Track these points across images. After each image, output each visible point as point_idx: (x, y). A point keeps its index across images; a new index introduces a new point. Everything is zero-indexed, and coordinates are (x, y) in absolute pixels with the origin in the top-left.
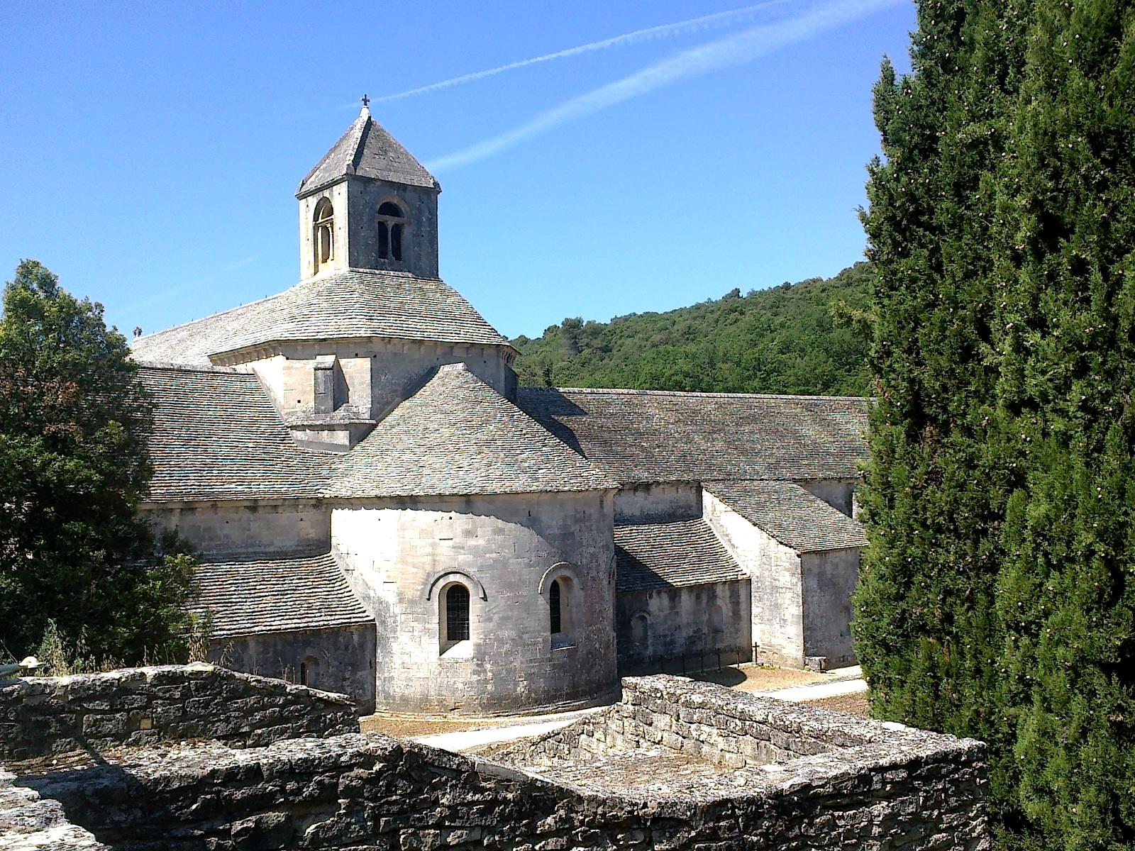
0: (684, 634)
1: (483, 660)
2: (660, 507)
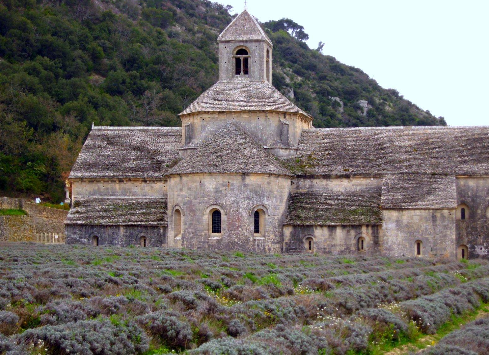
0: (338, 249)
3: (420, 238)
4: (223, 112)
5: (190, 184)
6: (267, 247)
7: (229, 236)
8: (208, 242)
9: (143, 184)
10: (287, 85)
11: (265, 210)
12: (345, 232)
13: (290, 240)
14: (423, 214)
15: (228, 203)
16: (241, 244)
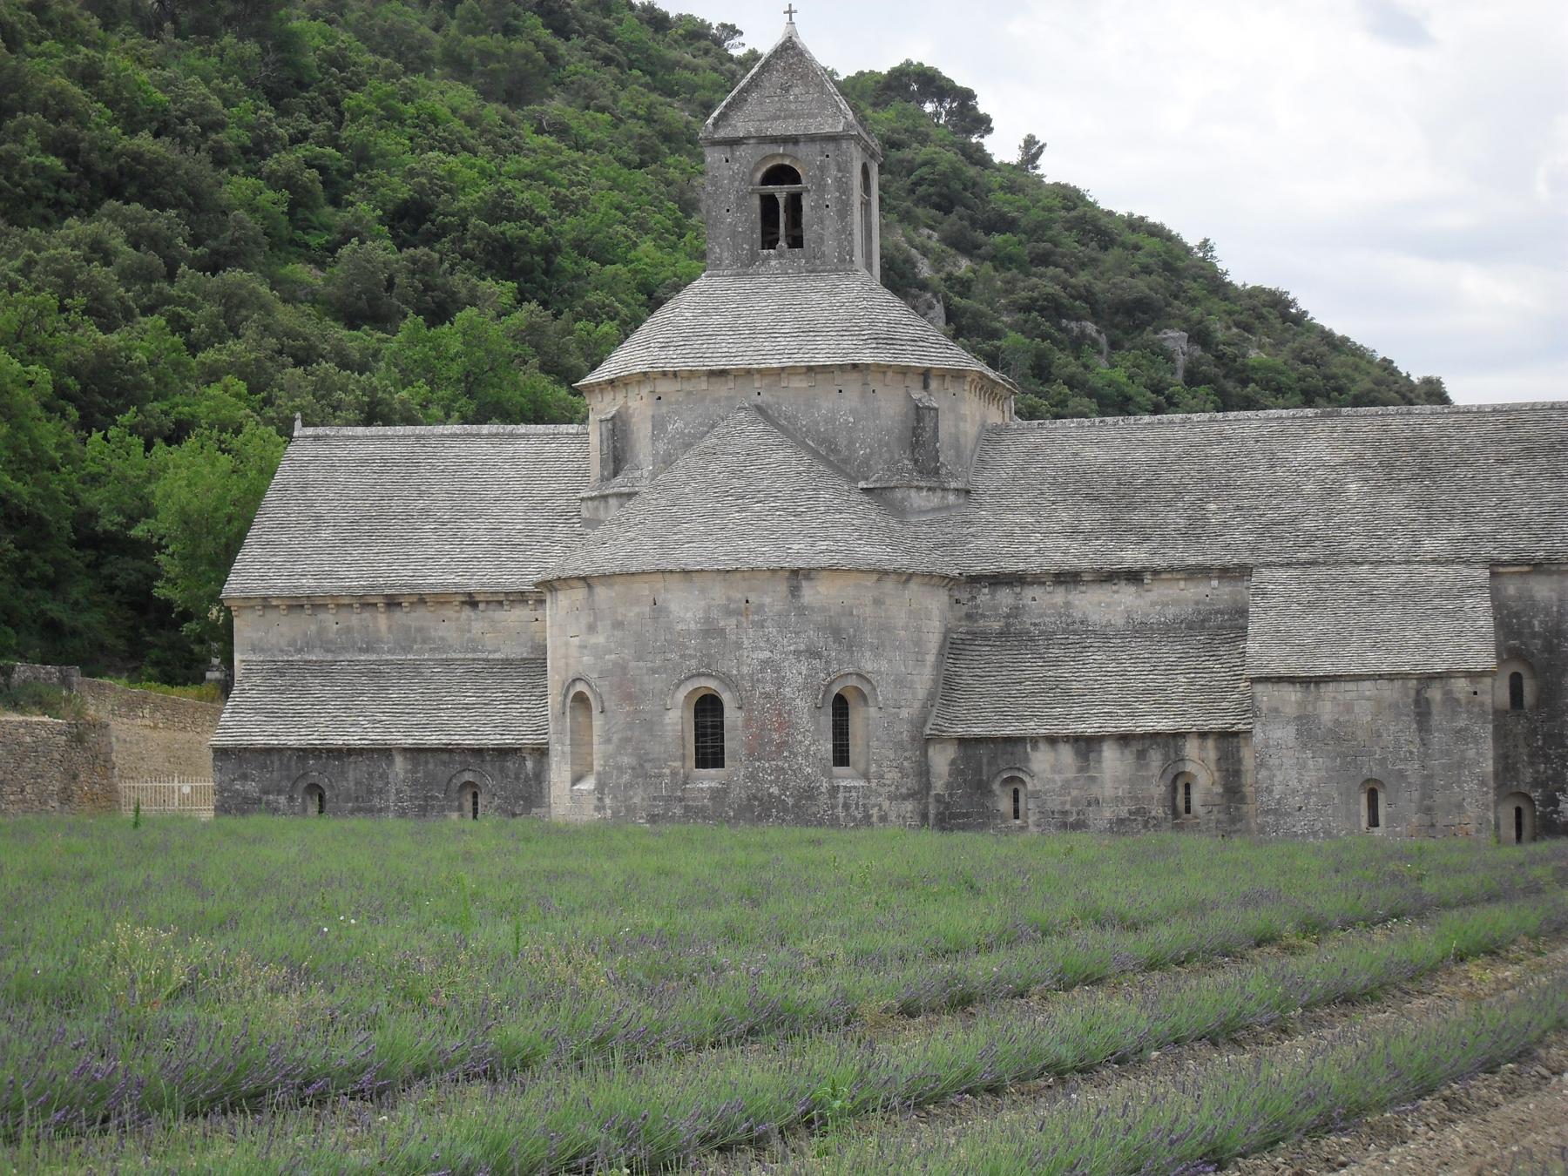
0: (1108, 814)
1: (602, 793)
2: (1171, 612)
3: (1377, 771)
4: (723, 373)
5: (620, 610)
6: (874, 811)
7: (752, 777)
8: (681, 800)
9: (467, 612)
10: (924, 286)
11: (866, 689)
12: (1130, 755)
13: (949, 786)
14: (1387, 694)
15: (745, 670)
16: (790, 801)
